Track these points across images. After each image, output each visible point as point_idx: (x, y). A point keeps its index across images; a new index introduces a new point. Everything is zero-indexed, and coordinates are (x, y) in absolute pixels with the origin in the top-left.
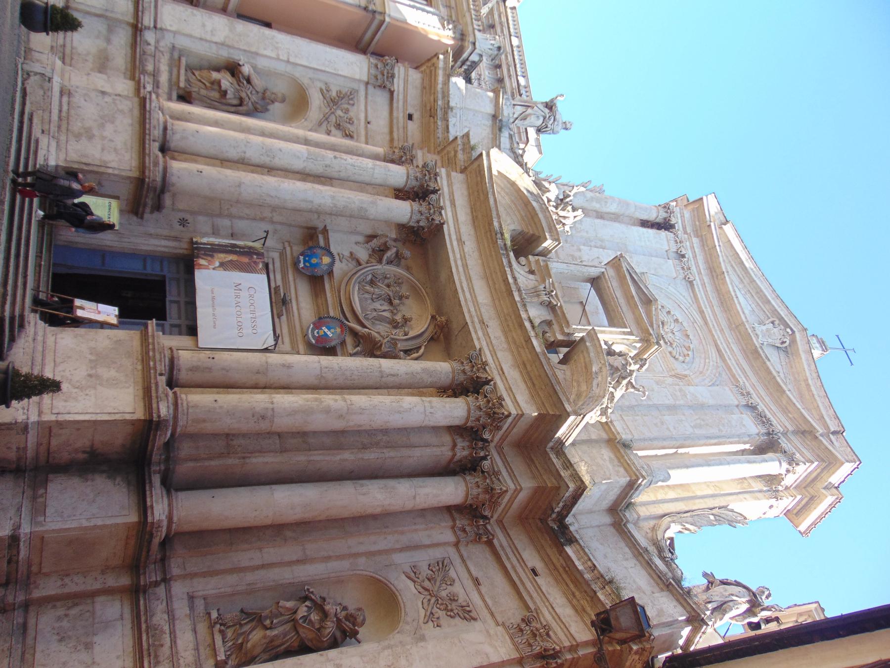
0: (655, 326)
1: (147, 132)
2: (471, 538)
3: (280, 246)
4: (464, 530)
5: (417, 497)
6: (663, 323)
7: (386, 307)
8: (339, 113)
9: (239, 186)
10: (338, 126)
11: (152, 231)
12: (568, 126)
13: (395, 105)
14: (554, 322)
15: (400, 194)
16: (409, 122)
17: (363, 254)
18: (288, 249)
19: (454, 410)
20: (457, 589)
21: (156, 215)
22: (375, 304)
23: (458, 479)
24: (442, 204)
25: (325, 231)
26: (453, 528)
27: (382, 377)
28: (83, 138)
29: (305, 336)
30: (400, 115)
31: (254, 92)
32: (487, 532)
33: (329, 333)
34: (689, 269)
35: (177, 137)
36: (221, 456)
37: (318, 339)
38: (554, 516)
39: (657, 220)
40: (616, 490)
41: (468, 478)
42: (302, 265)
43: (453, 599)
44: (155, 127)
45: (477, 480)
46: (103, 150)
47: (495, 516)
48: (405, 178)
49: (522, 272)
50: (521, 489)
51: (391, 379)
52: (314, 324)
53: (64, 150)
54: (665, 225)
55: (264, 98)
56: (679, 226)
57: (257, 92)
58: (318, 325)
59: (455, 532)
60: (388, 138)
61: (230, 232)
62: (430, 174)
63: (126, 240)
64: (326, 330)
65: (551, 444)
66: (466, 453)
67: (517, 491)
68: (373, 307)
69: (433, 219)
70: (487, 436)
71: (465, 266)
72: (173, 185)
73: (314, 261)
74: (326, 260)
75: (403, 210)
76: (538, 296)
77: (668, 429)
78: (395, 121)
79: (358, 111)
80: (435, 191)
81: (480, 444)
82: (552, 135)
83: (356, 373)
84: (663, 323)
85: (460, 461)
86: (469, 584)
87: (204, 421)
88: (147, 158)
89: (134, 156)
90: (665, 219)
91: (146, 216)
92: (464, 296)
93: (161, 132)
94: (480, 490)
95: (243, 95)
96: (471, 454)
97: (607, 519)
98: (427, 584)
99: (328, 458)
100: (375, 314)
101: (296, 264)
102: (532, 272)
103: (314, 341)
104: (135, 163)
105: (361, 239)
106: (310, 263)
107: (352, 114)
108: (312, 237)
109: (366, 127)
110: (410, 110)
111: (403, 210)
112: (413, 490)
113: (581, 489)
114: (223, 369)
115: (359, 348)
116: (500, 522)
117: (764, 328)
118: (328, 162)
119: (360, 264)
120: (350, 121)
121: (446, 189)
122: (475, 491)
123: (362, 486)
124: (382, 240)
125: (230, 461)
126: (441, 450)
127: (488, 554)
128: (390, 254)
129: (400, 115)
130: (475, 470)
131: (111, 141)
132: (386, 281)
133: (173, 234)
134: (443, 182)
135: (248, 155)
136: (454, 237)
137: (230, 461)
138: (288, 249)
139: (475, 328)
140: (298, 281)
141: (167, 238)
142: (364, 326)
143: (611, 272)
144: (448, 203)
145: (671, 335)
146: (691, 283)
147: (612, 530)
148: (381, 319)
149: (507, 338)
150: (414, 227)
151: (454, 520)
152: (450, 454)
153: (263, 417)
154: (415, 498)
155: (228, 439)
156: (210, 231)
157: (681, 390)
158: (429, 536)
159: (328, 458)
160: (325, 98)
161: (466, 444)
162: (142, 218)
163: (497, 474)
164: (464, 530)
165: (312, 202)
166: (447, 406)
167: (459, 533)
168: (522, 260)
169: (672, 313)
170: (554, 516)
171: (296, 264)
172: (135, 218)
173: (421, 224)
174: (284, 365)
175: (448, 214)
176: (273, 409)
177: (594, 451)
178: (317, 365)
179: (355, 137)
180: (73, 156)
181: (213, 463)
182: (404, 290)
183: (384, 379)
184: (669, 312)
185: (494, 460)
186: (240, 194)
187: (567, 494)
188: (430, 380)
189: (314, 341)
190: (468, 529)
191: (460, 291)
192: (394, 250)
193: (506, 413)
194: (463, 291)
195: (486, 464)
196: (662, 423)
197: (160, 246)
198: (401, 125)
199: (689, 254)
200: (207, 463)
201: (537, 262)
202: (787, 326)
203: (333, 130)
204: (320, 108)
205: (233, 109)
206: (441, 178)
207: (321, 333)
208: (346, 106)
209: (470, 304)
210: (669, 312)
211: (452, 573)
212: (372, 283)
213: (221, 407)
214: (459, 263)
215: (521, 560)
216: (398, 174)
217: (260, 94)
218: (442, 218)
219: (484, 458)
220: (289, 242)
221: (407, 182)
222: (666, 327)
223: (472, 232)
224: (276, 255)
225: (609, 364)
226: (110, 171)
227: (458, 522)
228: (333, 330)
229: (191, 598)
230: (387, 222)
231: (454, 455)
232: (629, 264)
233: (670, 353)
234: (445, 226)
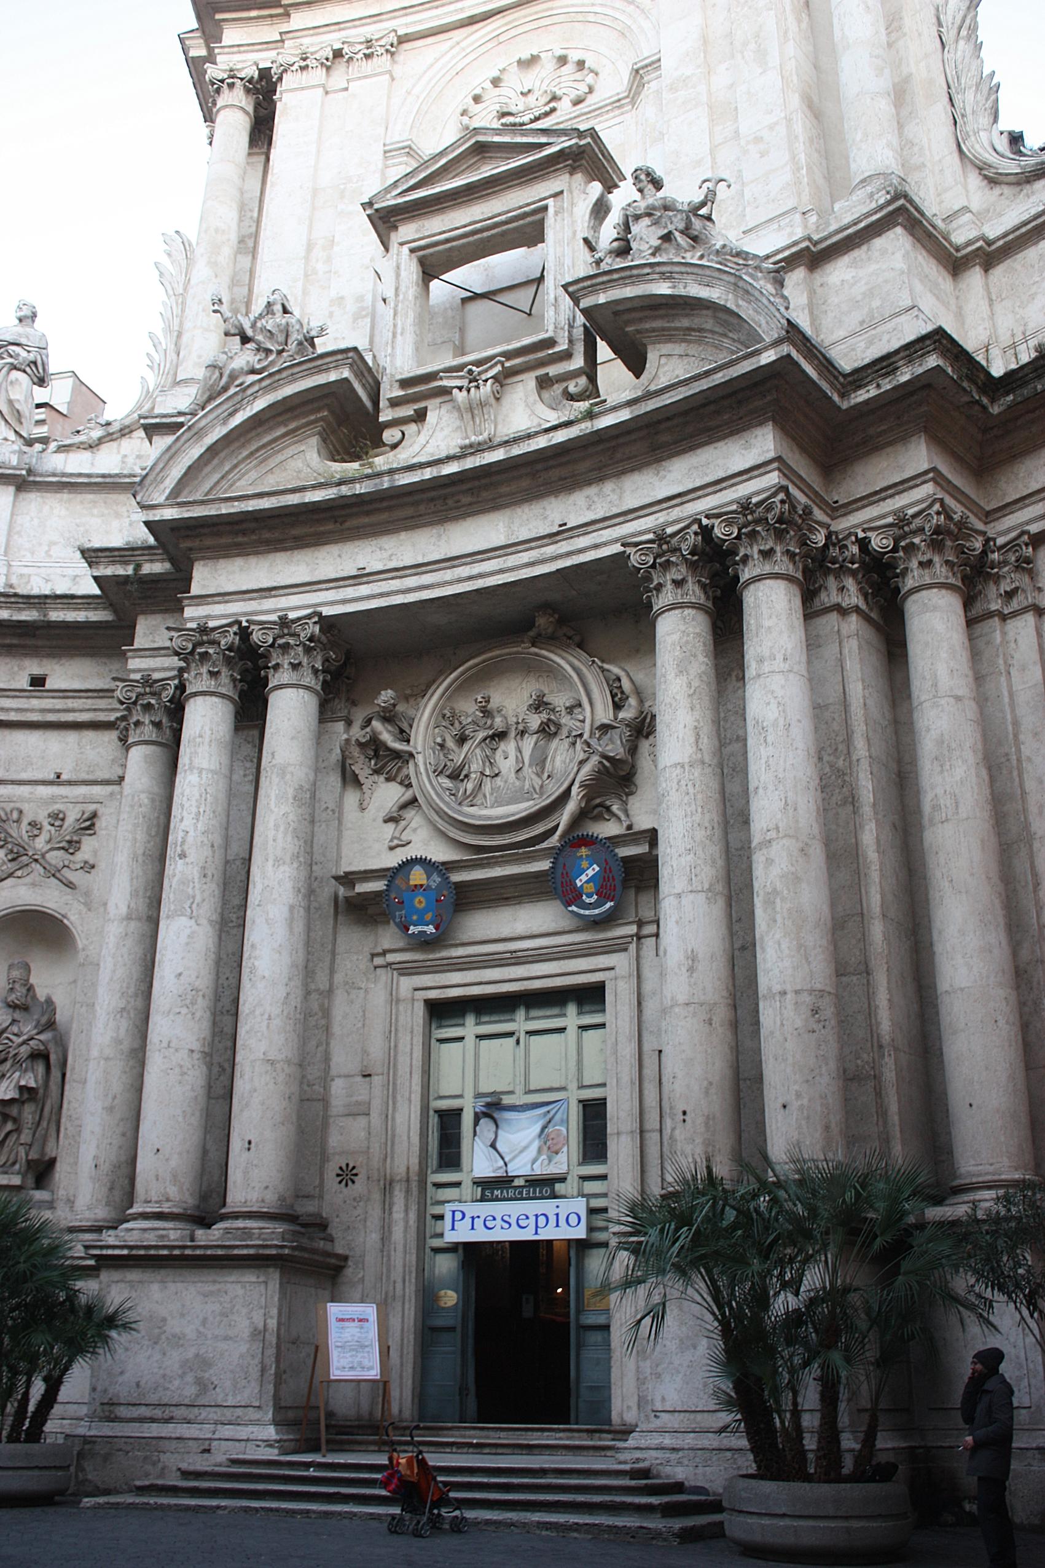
0: (544, 140)
1: (177, 1252)
2: (1027, 579)
3: (384, 975)
4: (1010, 595)
5: (960, 693)
6: (504, 114)
7: (509, 746)
8: (40, 843)
9: (272, 1063)
10: (72, 846)
11: (374, 1237)
12: (26, 312)
13: (13, 717)
14: (541, 372)
15: (250, 713)
16: (49, 685)
17: (387, 794)
18: (390, 958)
19: (771, 608)
21: (334, 1230)
22: (504, 771)
23: (912, 606)
24: (274, 617)
25: (348, 879)
26: (1004, 618)
27: (703, 763)
28: (207, 1375)
29: (596, 924)
30: (36, 707)
31: (15, 1029)
32: (1012, 545)
33: (590, 873)
34: (369, 42)
35: (173, 1191)
36: (879, 1093)
37: (603, 895)
38: (985, 401)
39: (250, 109)
40: (920, 258)
41: (910, 583)
42: (430, 929)
44: (162, 1237)
45: (914, 564)
46: (227, 1338)
47: (980, 526)
48: (215, 699)
49: (422, 439)
50: (933, 469)
51: (705, 741)
52: (568, 904)
53: (239, 1412)
54: (264, 91)
55: (25, 1008)
56: (265, 59)
57: (14, 1021)
58: (571, 896)
59: (1015, 614)
60: (90, 735)
61: (359, 1079)
62: (201, 644)
63: (399, 1286)
64: (584, 878)
65: (836, 398)
66: (850, 583)
67: (938, 478)
68: (513, 775)
69: (311, 640)
70: (819, 538)
71: (418, 568)
72: (282, 1199)
73: (419, 901)
74: (418, 876)
75: (290, 709)
76: (482, 405)
77: (771, 128)
78: (51, 717)
79: (36, 803)
80: (244, 633)
81: (834, 552)
82: (51, 350)
83: (697, 818)
84: (504, 114)
85: (865, 596)
87: (827, 1128)
88: (236, 1252)
89: (232, 1278)
90: (248, 91)
91: (340, 1250)
92: (495, 574)
93: (170, 1225)
94: (936, 559)
95: (24, 1051)
96: (853, 573)
97: (975, 276)
99: (875, 876)
100: (528, 771)
101: (426, 943)
102: (420, 417)
103: (609, 905)
104: (250, 1277)
105: (351, 798)
106: (425, 911)
107: (42, 817)
108: (359, 905)
109: (70, 783)
110: (24, 683)
111: (290, 709)
112: (943, 702)
113: (938, 339)
114: (707, 1093)
115: (615, 808)
116: (989, 516)
118: (195, 873)
119: (414, 800)
120: (57, 817)
121: (235, 608)
122: (941, 572)
123: (936, 807)
124: (356, 752)
125: (889, 1074)
126: (852, 640)
128: (387, 736)
129: (36, 707)
130: (892, 566)
131: (204, 1322)
132: (450, 744)
133: (377, 1196)
134: (217, 614)
135: (196, 1046)
136: (350, 592)
137: (889, 1074)
138: (390, 958)
139: (569, 554)
140: (465, 938)
141: (387, 1207)
142: (567, 794)
143: (408, 231)
144: (269, 604)
145: (531, 99)
146: (403, 40)
147: (998, 271)
148: (540, 762)
149: (589, 483)
150: (325, 682)
151: (990, 615)
152: (854, 618)
153: (815, 1011)
154: (958, 699)
155: (855, 1079)
156: (362, 1121)
157: (673, 89)
158: (1023, 669)
159: (875, 876)
160: (10, 875)
161: (832, 583)
162: (346, 1258)
163: (902, 520)
164: (1010, 595)
165: (292, 908)
166: (767, 623)
167: (1015, 604)
168: (390, 435)
169: (478, 91)
170: (985, 401)
171: (426, 943)
172: (349, 1272)
173: (319, 665)
174: (691, 970)
175: (296, 605)
176: (797, 992)
177: (834, 300)
178: (687, 900)
179: (92, 807)
180: (249, 1392)
181: (893, 1107)
182: (468, 708)
183: (707, 759)
184: (477, 99)
185: (868, 521)
186: (288, 1062)
187: (949, 370)
188: (701, 658)
189: (609, 905)
190: (1005, 586)
192: (376, 724)
193: (781, 496)
194: (481, 576)
195: (878, 542)
196: (758, 140)
197: (407, 1222)
198: (59, 704)
199: (334, 40)
200: (895, 1118)
201: (394, 403)
203: (80, 856)
204: (34, 885)
205: (56, 1073)
206: (208, 617)
207: (590, 888)
208: (24, 826)
209: (512, 561)
210: (477, 99)
212: (456, 776)
213: (798, 1095)
214: (412, 582)
216: (207, 719)
217: (17, 1015)
218: (309, 617)
219: (863, 544)
220: (373, 955)
221: (222, 696)
222: (513, 109)
223: (334, 549)
224: (406, 984)
225: (653, 254)
226: (273, 1323)
227: (994, 607)
228: (585, 864)
230: (320, 737)
231: (857, 609)
232: (387, 190)
233: (577, 102)
234: (327, 611)
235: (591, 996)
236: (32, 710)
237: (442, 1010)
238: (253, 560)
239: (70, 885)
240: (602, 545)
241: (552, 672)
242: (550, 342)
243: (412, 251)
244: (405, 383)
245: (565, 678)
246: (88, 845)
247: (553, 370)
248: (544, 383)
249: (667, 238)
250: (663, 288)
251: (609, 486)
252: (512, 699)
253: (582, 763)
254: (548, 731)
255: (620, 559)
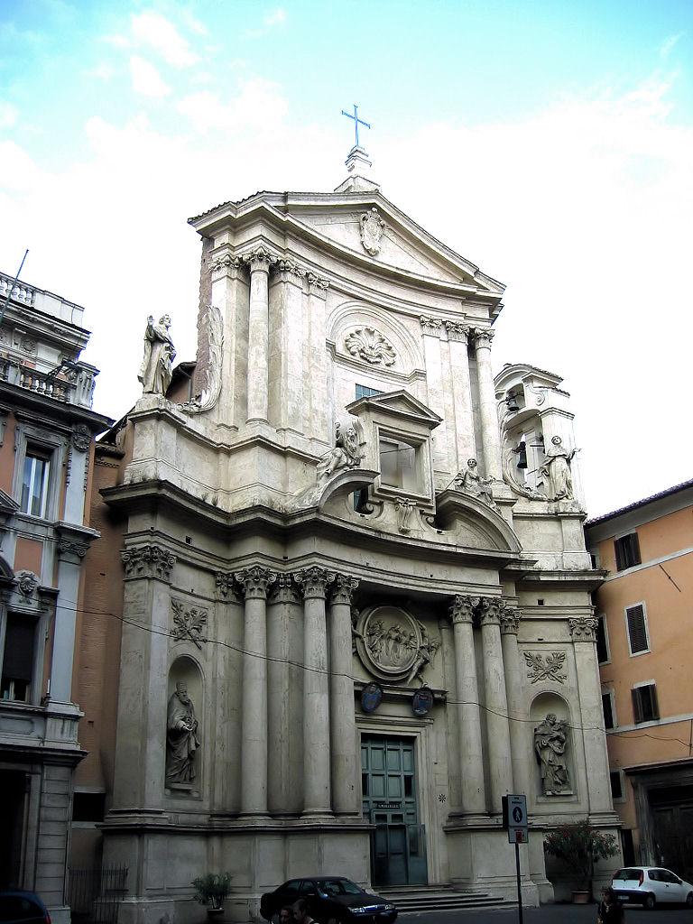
20: (544, 655)
43: (548, 659)
78: (194, 562)
79: (188, 603)
86: (541, 647)
92: (412, 586)
98: (540, 671)
117: (365, 232)
127: (525, 624)
148: (396, 650)
184: (352, 335)
191: (407, 587)
202: (370, 206)
209: (418, 583)
211: (534, 654)
215: (533, 607)
222: (366, 351)
229: (538, 803)
233: (388, 365)
234: (363, 578)
235: (410, 741)
236: (189, 556)
237: (366, 738)
238: (333, 544)
239: (200, 648)
240: (447, 590)
241: (402, 618)
242: (428, 501)
243: (380, 429)
244: (380, 490)
245: (410, 625)
246: (204, 628)
247: (426, 511)
248: (421, 512)
249: (482, 493)
250: (478, 510)
251: (445, 568)
252: (387, 624)
253: (418, 659)
254: (397, 640)
255: (453, 597)
